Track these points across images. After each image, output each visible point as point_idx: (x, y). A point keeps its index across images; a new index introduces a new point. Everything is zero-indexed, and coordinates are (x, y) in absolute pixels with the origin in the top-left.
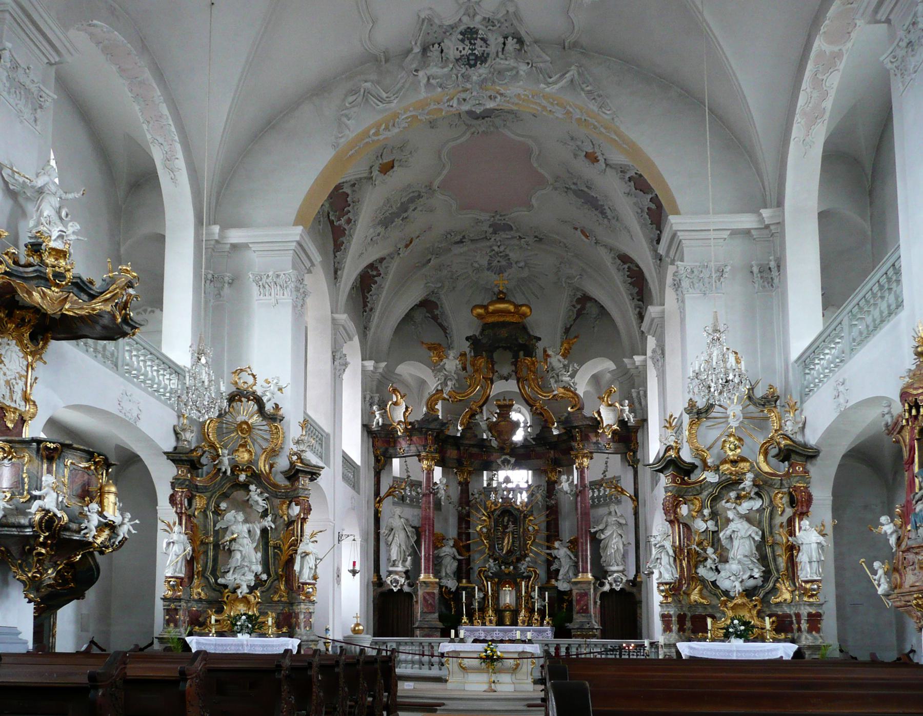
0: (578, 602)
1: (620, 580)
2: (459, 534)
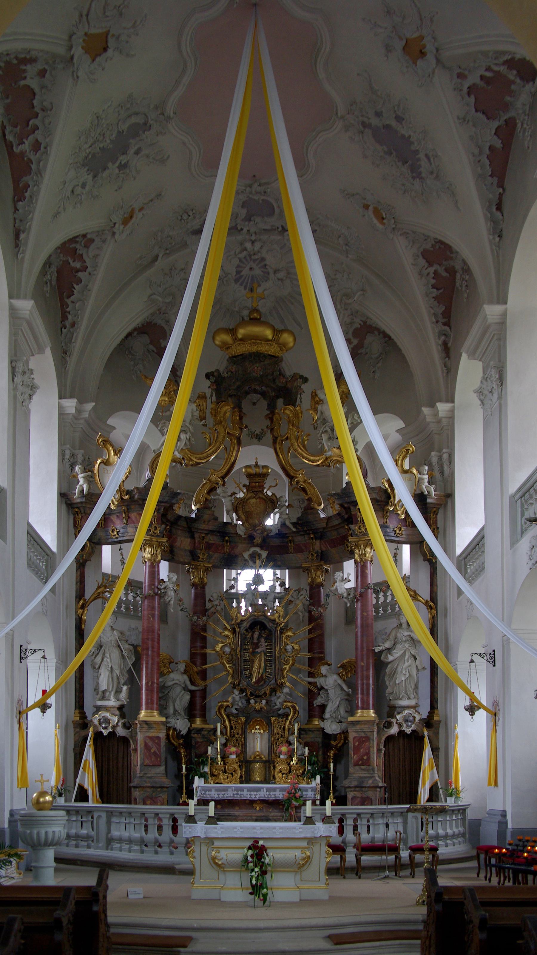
0: (356, 749)
1: (411, 718)
2: (193, 656)
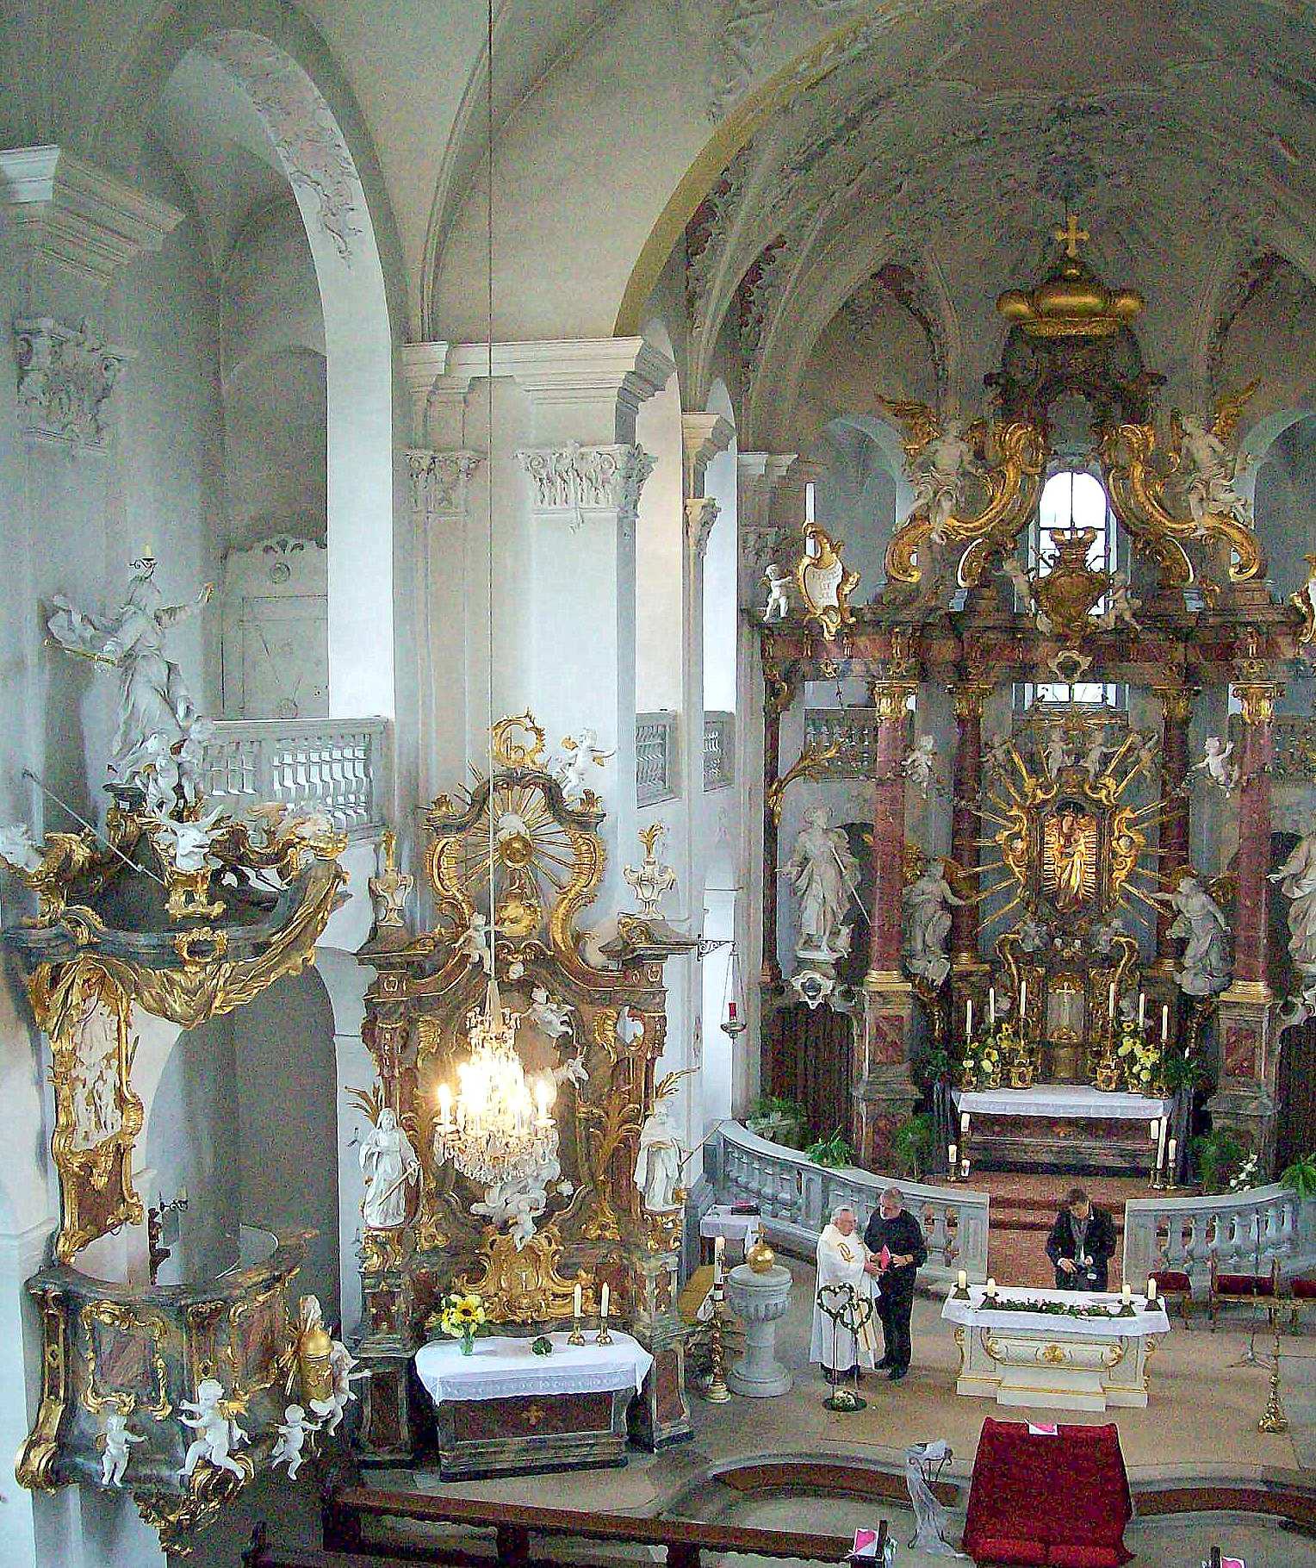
0: (1231, 1049)
